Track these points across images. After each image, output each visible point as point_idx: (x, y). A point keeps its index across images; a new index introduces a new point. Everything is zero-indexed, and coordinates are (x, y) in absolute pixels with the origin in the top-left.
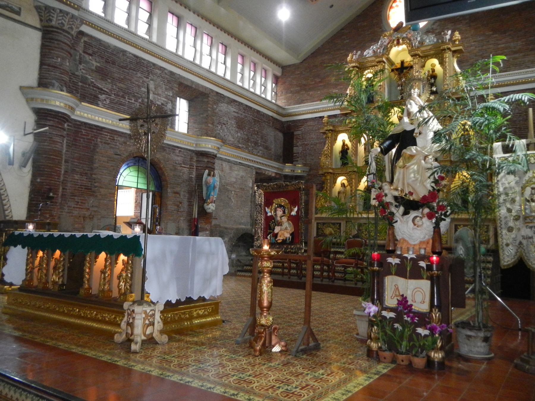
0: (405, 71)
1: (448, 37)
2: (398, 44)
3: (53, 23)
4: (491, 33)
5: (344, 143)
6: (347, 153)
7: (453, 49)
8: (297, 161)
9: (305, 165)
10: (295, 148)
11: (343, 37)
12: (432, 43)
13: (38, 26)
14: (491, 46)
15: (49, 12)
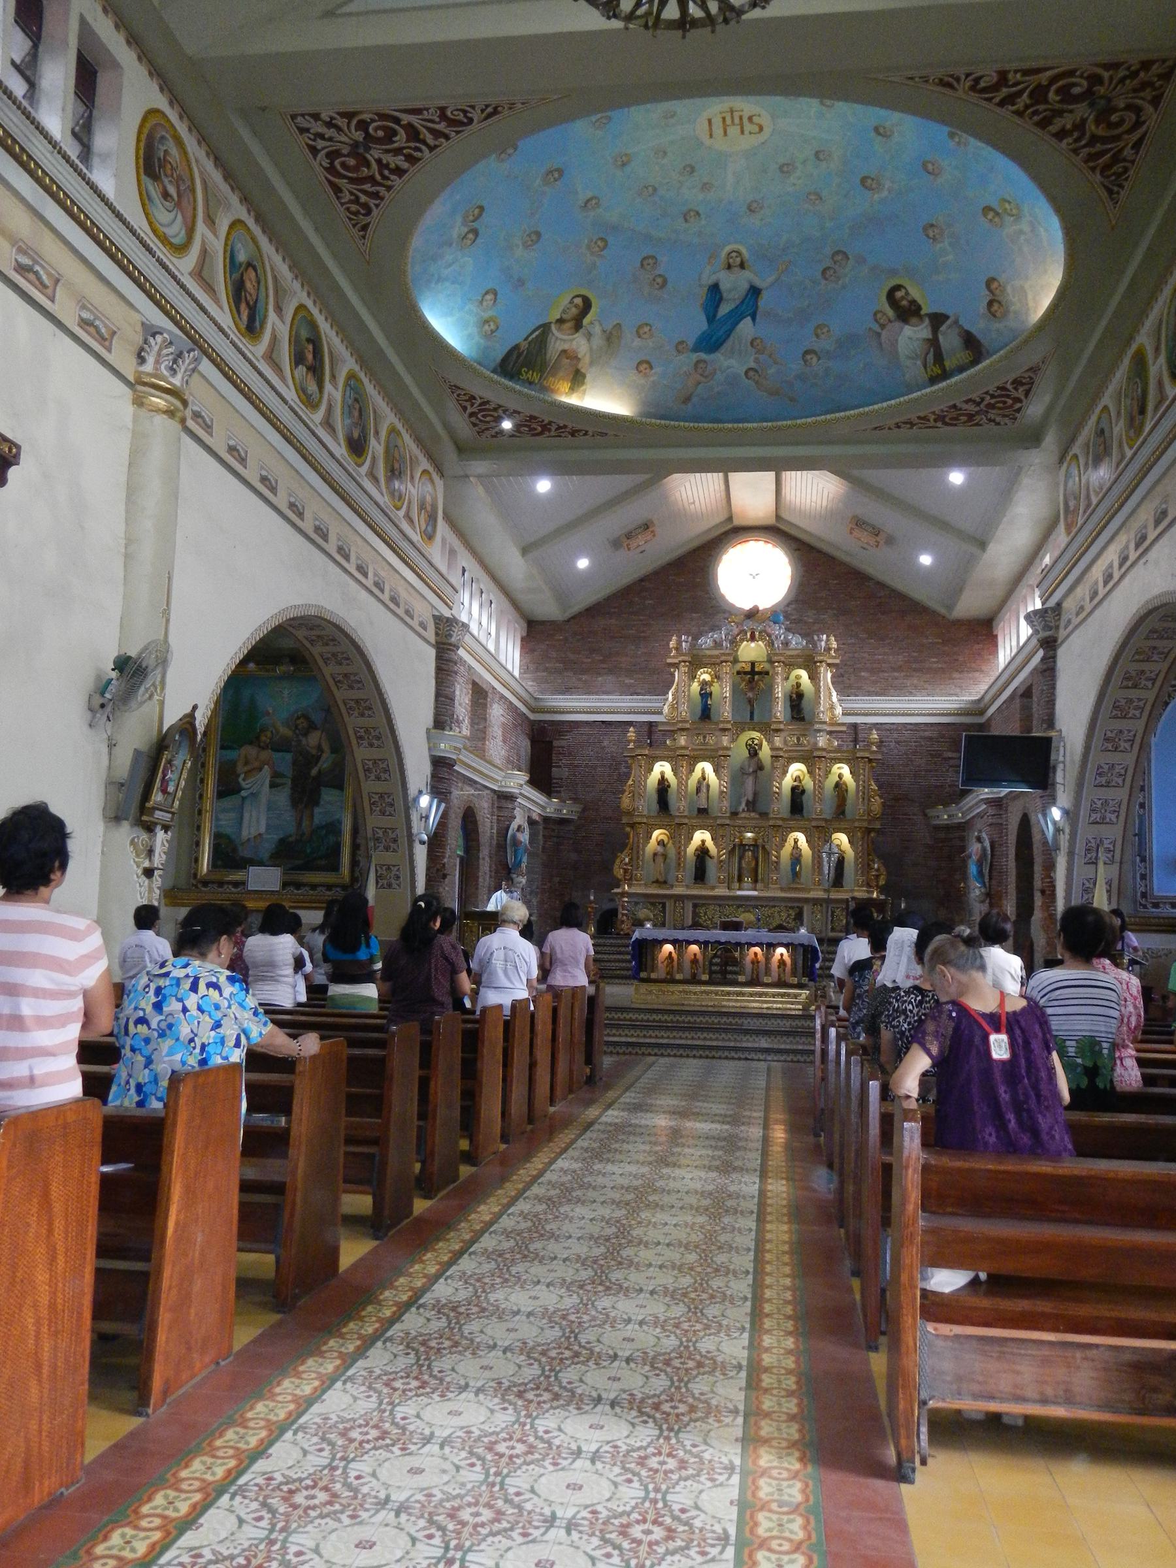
0: (756, 677)
1: (823, 644)
2: (753, 638)
3: (453, 640)
4: (865, 636)
5: (663, 777)
6: (667, 791)
7: (830, 661)
8: (559, 792)
9: (575, 800)
10: (554, 769)
11: (644, 594)
12: (800, 647)
13: (433, 642)
14: (866, 655)
15: (451, 625)
